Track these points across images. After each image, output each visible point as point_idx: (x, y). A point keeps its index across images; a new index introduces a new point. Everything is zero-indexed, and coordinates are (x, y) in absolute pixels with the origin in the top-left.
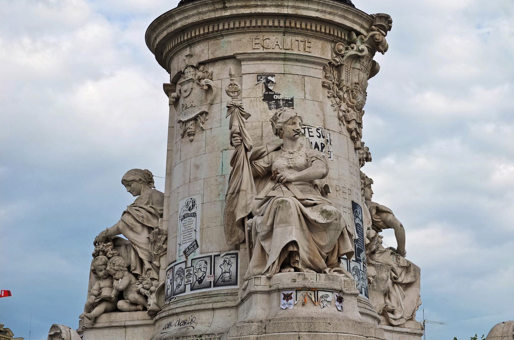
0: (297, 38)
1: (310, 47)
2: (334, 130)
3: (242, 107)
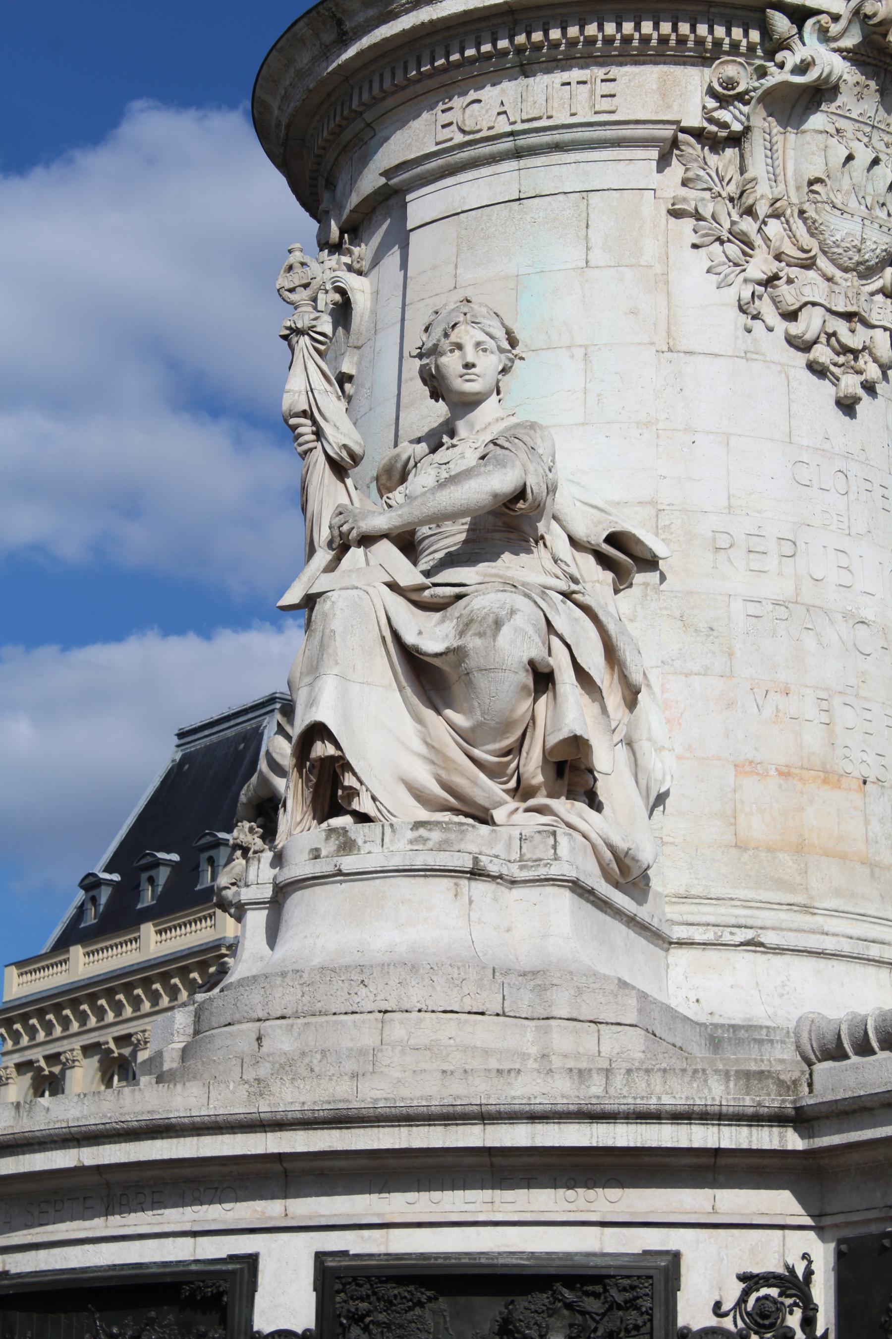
0: (566, 76)
1: (613, 96)
2: (716, 351)
3: (318, 329)
